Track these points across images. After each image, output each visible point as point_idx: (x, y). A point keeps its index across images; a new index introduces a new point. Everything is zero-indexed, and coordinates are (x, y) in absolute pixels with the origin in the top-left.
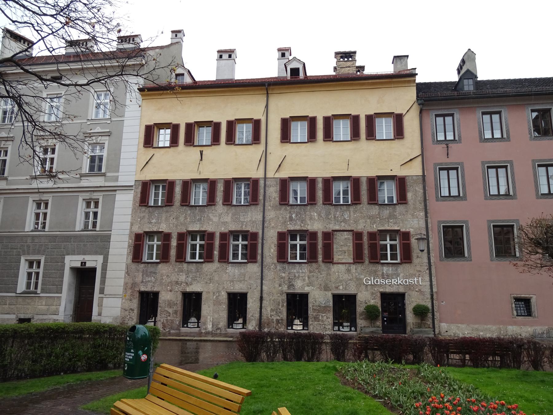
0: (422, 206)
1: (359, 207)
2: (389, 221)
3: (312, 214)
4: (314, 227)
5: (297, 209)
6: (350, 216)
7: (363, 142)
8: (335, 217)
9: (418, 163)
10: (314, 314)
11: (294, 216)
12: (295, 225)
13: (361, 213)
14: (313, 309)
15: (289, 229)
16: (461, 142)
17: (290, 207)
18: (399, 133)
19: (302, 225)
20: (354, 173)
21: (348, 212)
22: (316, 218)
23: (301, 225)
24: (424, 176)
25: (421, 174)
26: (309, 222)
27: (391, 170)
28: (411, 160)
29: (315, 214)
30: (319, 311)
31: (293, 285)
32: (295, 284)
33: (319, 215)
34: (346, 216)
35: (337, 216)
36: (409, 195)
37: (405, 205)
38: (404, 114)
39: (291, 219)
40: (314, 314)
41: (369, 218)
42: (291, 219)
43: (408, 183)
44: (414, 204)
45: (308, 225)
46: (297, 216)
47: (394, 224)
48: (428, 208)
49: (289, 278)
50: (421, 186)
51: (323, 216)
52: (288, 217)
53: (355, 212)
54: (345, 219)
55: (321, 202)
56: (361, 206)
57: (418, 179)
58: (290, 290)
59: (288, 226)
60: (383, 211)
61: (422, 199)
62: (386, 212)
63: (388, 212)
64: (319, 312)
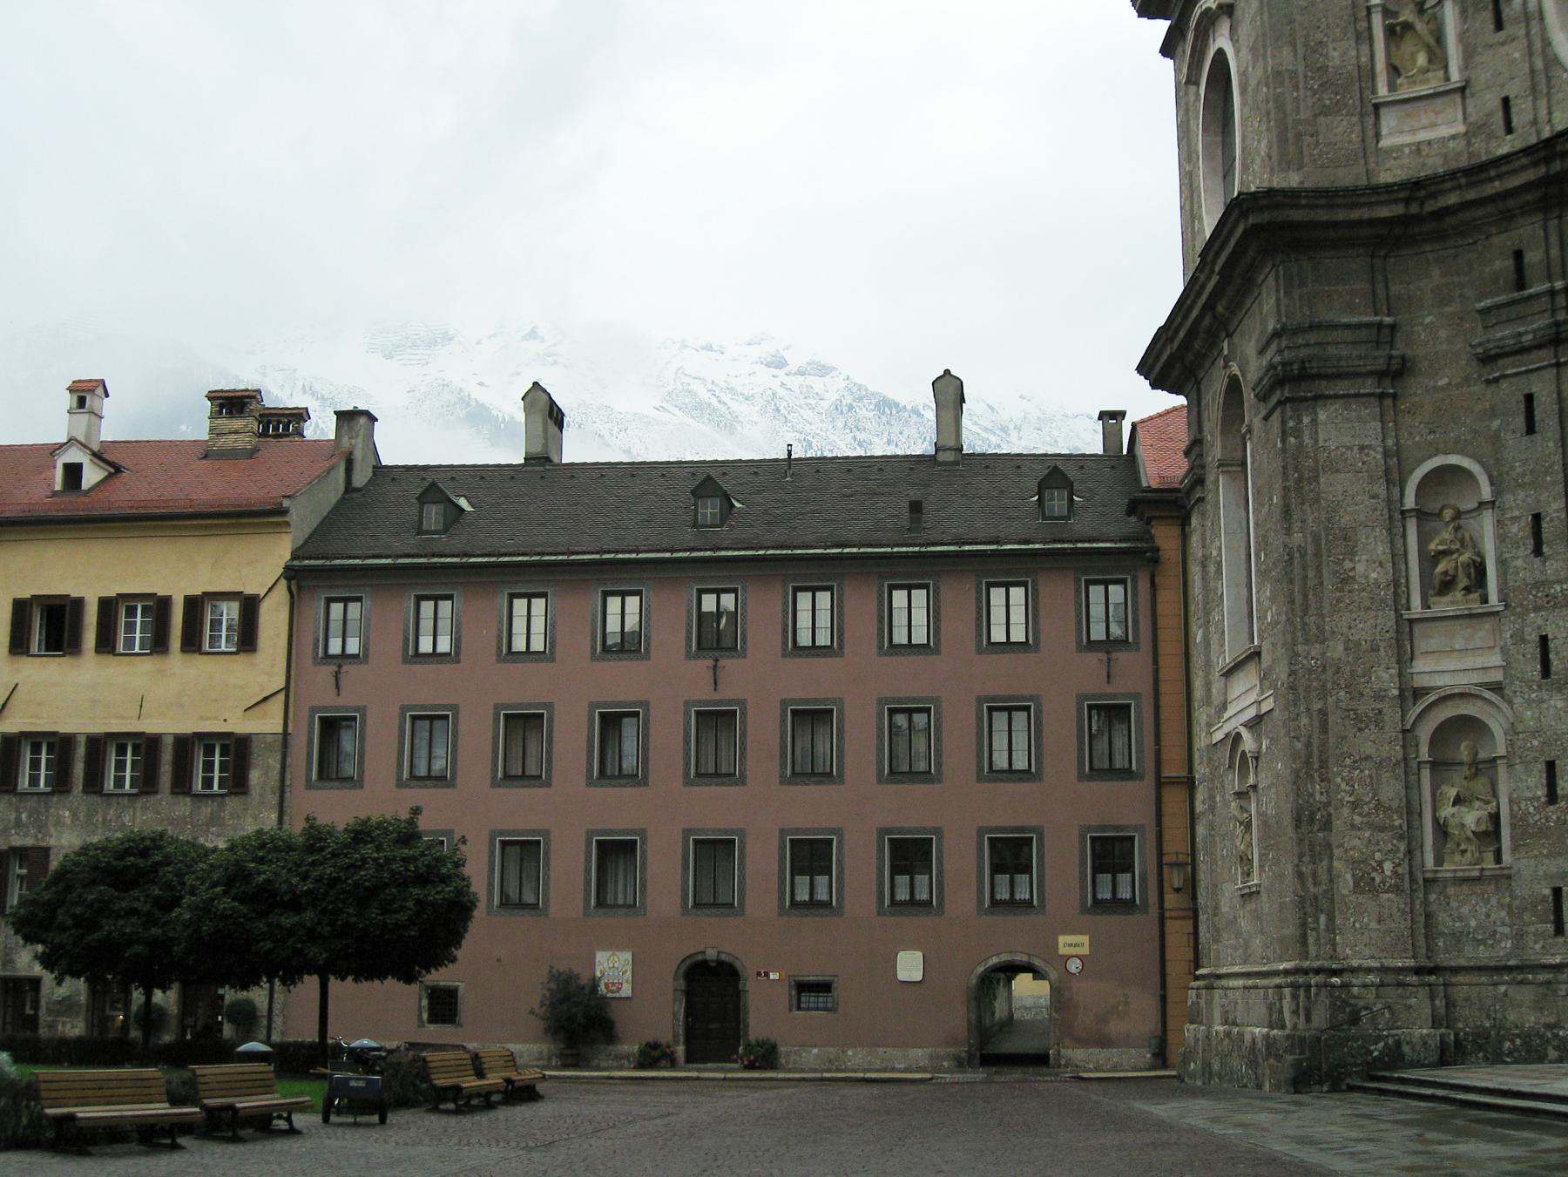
0: (275, 800)
1: (152, 798)
2: (208, 831)
3: (61, 813)
4: (63, 841)
5: (31, 803)
6: (134, 820)
7: (176, 658)
8: (104, 819)
9: (277, 704)
10: (49, 1019)
11: (24, 816)
12: (25, 835)
13: (158, 813)
14: (47, 1009)
15: (14, 844)
16: (367, 663)
17: (18, 797)
18: (247, 639)
19: (40, 836)
20: (150, 726)
21: (131, 810)
22: (68, 821)
23: (36, 836)
24: (285, 734)
25: (280, 730)
26: (52, 830)
27: (225, 720)
28: (265, 699)
29: (67, 814)
30: (59, 1014)
31: (11, 961)
32: (16, 957)
33: (74, 815)
34: (126, 819)
35: (109, 817)
36: (255, 776)
37: (243, 797)
38: (262, 595)
39: (18, 823)
40: (49, 1019)
41: (172, 824)
42: (18, 823)
43: (256, 748)
44: (261, 795)
45: (51, 836)
46: (29, 817)
47: (218, 836)
48: (286, 804)
49: (6, 947)
50: (278, 757)
51: (82, 818)
52: (13, 817)
53: (145, 809)
54: (124, 824)
55: (81, 788)
56: (159, 797)
57: (275, 741)
58: (7, 970)
59: (12, 838)
60: (199, 808)
61: (277, 784)
62: (207, 810)
63: (209, 810)
64: (58, 1016)
